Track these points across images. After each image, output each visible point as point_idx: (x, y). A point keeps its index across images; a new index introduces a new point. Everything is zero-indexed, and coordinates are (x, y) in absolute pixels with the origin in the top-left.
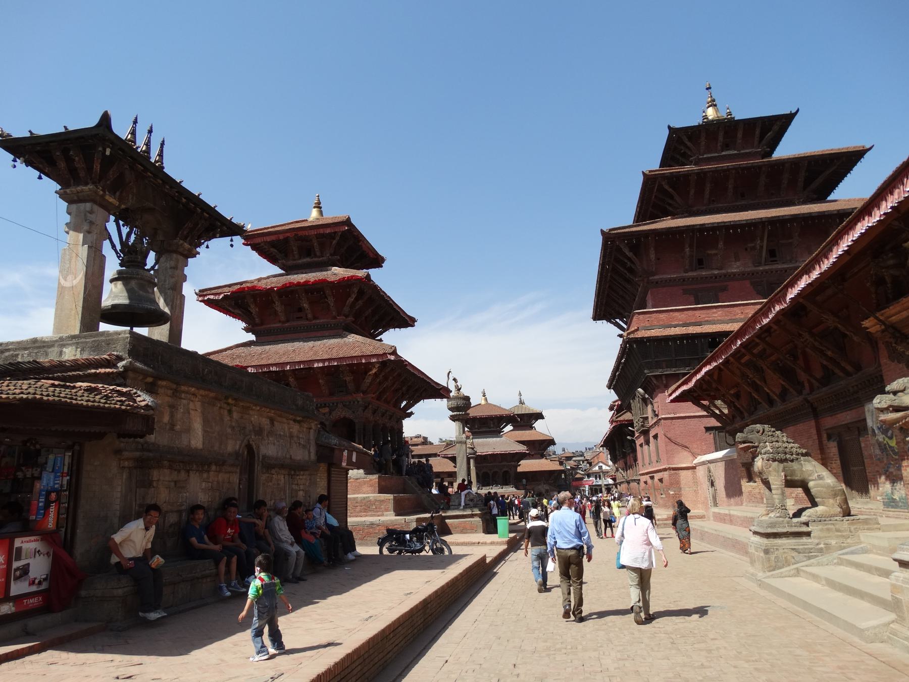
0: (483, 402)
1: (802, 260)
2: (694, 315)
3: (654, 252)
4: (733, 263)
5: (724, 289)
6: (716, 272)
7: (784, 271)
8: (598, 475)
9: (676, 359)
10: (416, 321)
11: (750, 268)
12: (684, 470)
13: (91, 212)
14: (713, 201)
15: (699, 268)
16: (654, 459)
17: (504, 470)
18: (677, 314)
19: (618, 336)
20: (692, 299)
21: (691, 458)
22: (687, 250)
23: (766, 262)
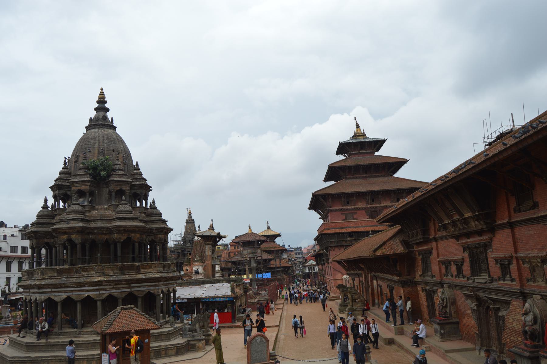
5: (356, 213)
6: (353, 207)
11: (365, 206)
14: (355, 173)
20: (344, 217)
22: (343, 199)
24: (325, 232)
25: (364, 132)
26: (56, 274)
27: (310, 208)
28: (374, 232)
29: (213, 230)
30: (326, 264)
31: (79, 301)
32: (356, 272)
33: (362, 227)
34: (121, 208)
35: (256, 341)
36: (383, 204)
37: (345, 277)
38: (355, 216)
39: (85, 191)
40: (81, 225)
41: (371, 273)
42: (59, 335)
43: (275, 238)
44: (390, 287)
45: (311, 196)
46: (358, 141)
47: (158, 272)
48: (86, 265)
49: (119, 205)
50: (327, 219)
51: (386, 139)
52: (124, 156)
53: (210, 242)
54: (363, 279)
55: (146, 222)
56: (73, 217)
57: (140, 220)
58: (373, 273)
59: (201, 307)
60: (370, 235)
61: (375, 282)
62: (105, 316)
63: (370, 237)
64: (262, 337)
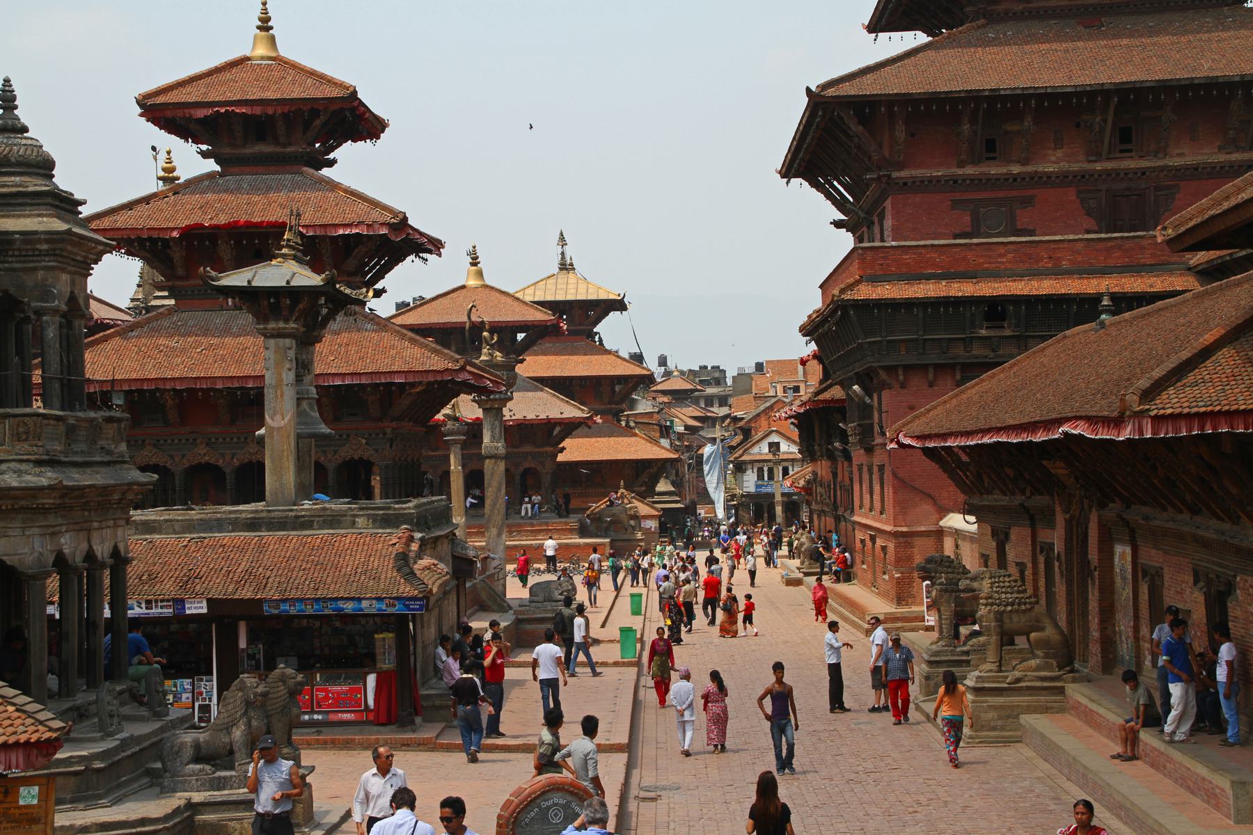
0: (472, 282)
3: (904, 128)
4: (1050, 152)
5: (1027, 202)
6: (1016, 169)
7: (1139, 174)
8: (766, 469)
9: (925, 340)
10: (443, 247)
11: (1075, 167)
12: (922, 536)
13: (289, 349)
15: (988, 159)
16: (877, 504)
17: (527, 465)
19: (831, 223)
21: (936, 516)
23: (1110, 152)
24: (865, 292)
28: (1124, 302)
30: (858, 455)
32: (1018, 499)
33: (1057, 273)
35: (544, 814)
36: (1179, 155)
37: (956, 521)
38: (1023, 220)
41: (1102, 506)
43: (598, 320)
44: (1209, 583)
47: (39, 463)
50: (877, 229)
54: (1056, 538)
58: (1114, 508)
59: (243, 644)
60: (1103, 316)
61: (1122, 552)
63: (1102, 324)
64: (572, 793)
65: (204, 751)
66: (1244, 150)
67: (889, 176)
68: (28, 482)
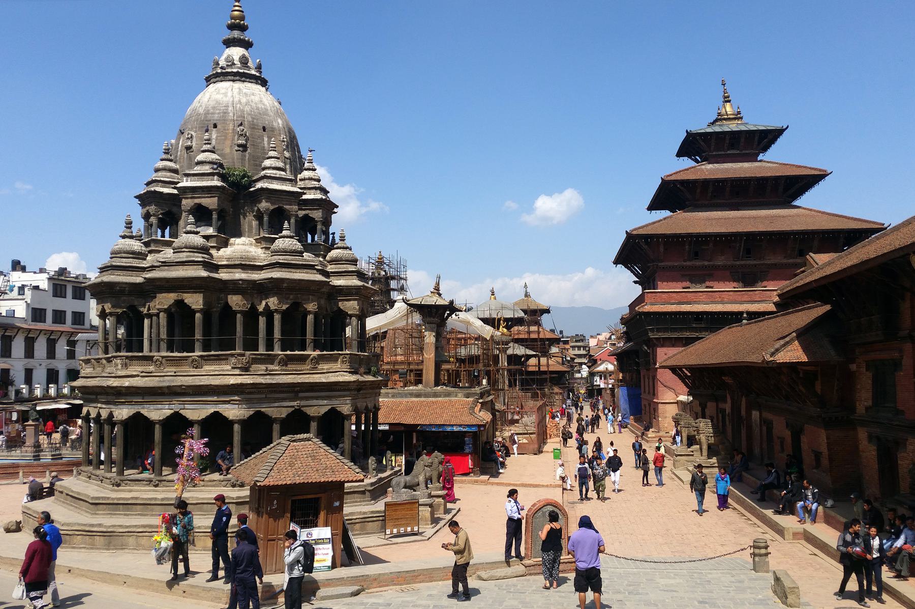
1: (768, 258)
2: (687, 296)
4: (719, 257)
6: (706, 263)
11: (729, 263)
15: (696, 259)
16: (651, 391)
18: (674, 295)
23: (742, 258)
25: (739, 113)
26: (152, 368)
27: (617, 262)
28: (753, 316)
29: (440, 295)
31: (198, 422)
33: (722, 302)
34: (280, 243)
39: (210, 208)
40: (204, 274)
42: (156, 486)
45: (624, 236)
46: (726, 129)
47: (350, 372)
48: (213, 353)
49: (277, 238)
50: (652, 284)
51: (784, 128)
52: (284, 141)
53: (434, 318)
54: (728, 407)
55: (326, 274)
56: (187, 257)
57: (318, 270)
59: (415, 441)
62: (257, 454)
65: (408, 484)
66: (794, 258)
67: (657, 265)
68: (347, 379)
